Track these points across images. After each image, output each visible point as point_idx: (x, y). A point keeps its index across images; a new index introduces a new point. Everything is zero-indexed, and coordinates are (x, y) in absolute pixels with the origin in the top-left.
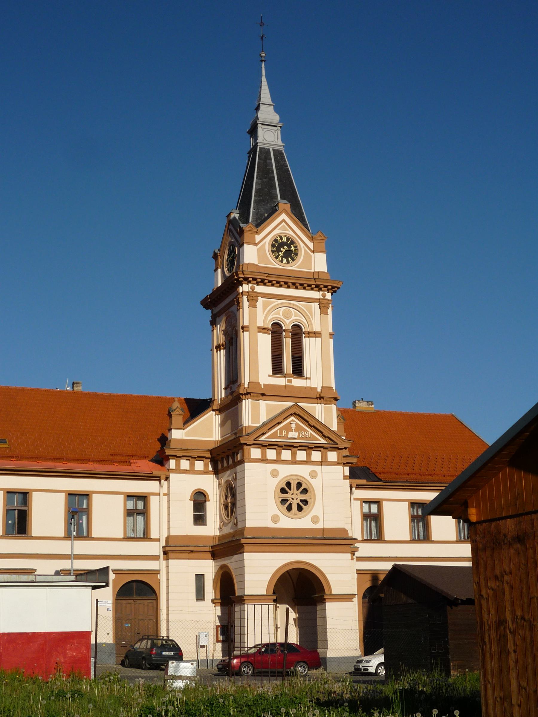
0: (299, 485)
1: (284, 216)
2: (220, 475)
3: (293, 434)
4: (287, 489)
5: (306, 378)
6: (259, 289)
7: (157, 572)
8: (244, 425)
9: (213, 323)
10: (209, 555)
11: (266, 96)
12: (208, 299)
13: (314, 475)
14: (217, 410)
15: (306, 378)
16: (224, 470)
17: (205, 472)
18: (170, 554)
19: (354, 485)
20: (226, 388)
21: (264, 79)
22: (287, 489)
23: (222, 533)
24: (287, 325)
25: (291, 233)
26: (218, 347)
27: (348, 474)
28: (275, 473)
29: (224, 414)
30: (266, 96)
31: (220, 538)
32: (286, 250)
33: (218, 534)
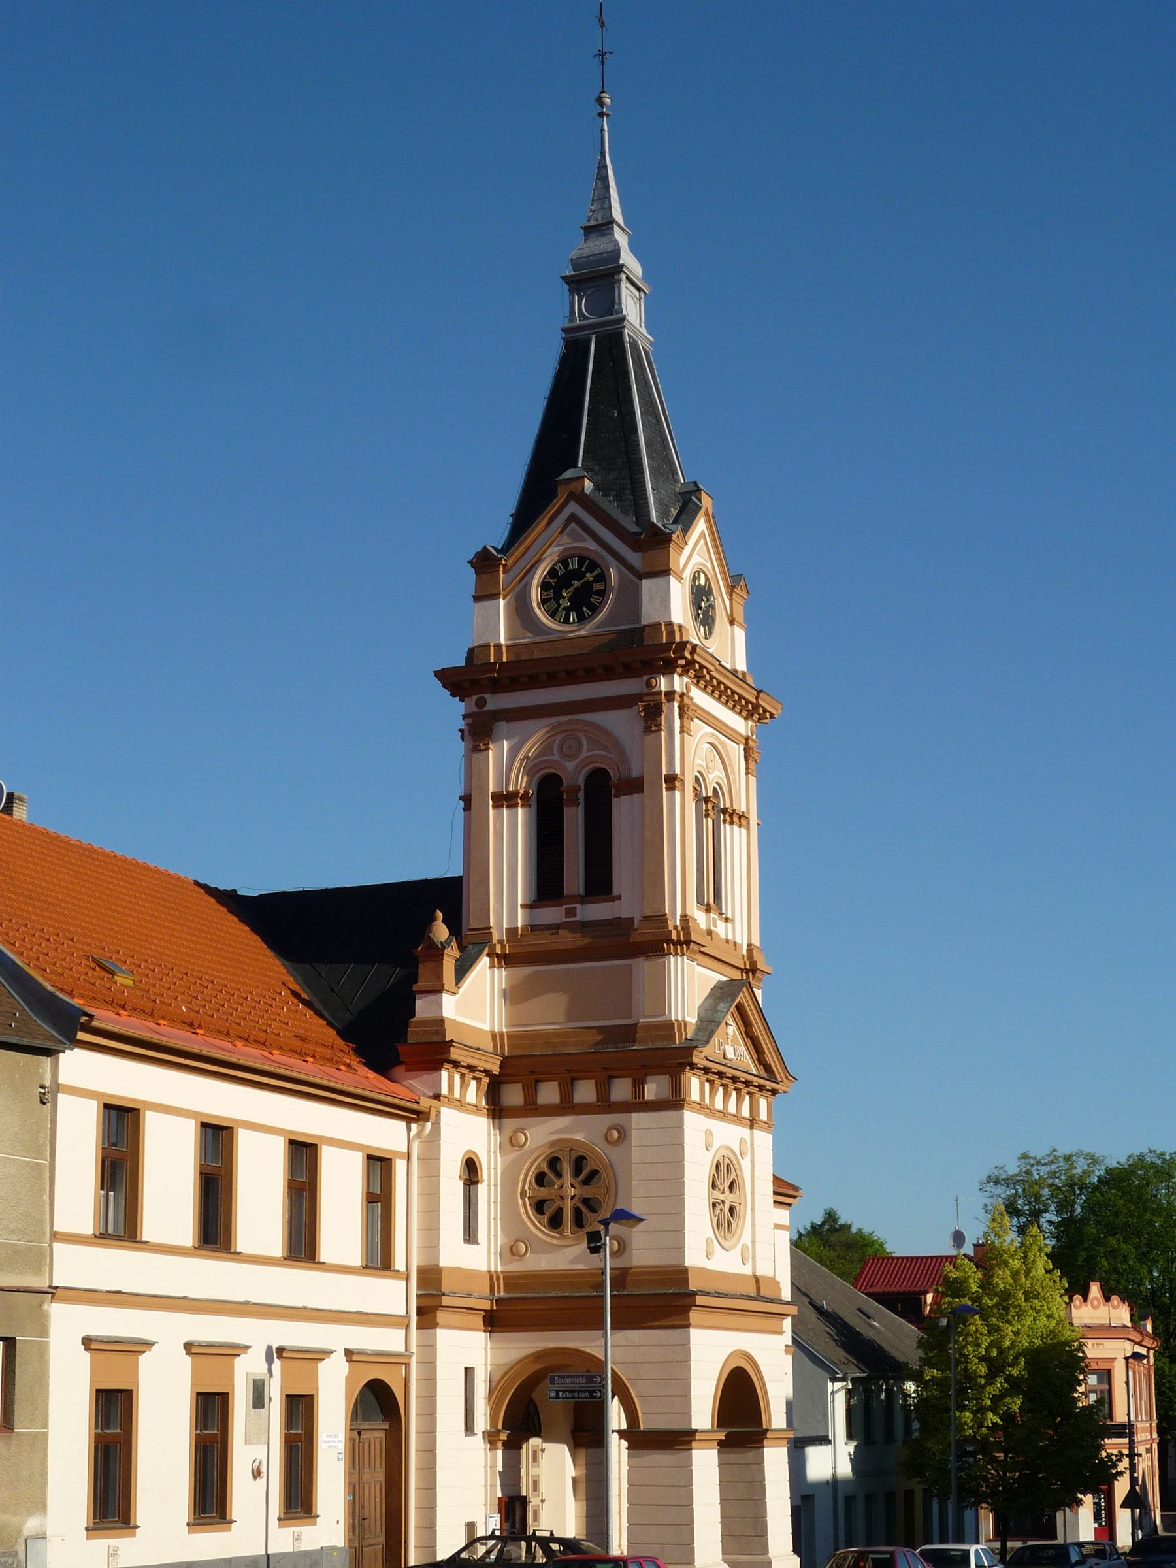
2: (511, 1123)
5: (727, 920)
7: (399, 1360)
8: (673, 1018)
9: (479, 732)
10: (479, 1320)
12: (494, 670)
14: (498, 955)
15: (727, 920)
16: (532, 1109)
17: (474, 1109)
18: (441, 1316)
20: (529, 907)
23: (516, 1267)
26: (505, 799)
29: (523, 971)
31: (511, 1281)
33: (499, 1269)
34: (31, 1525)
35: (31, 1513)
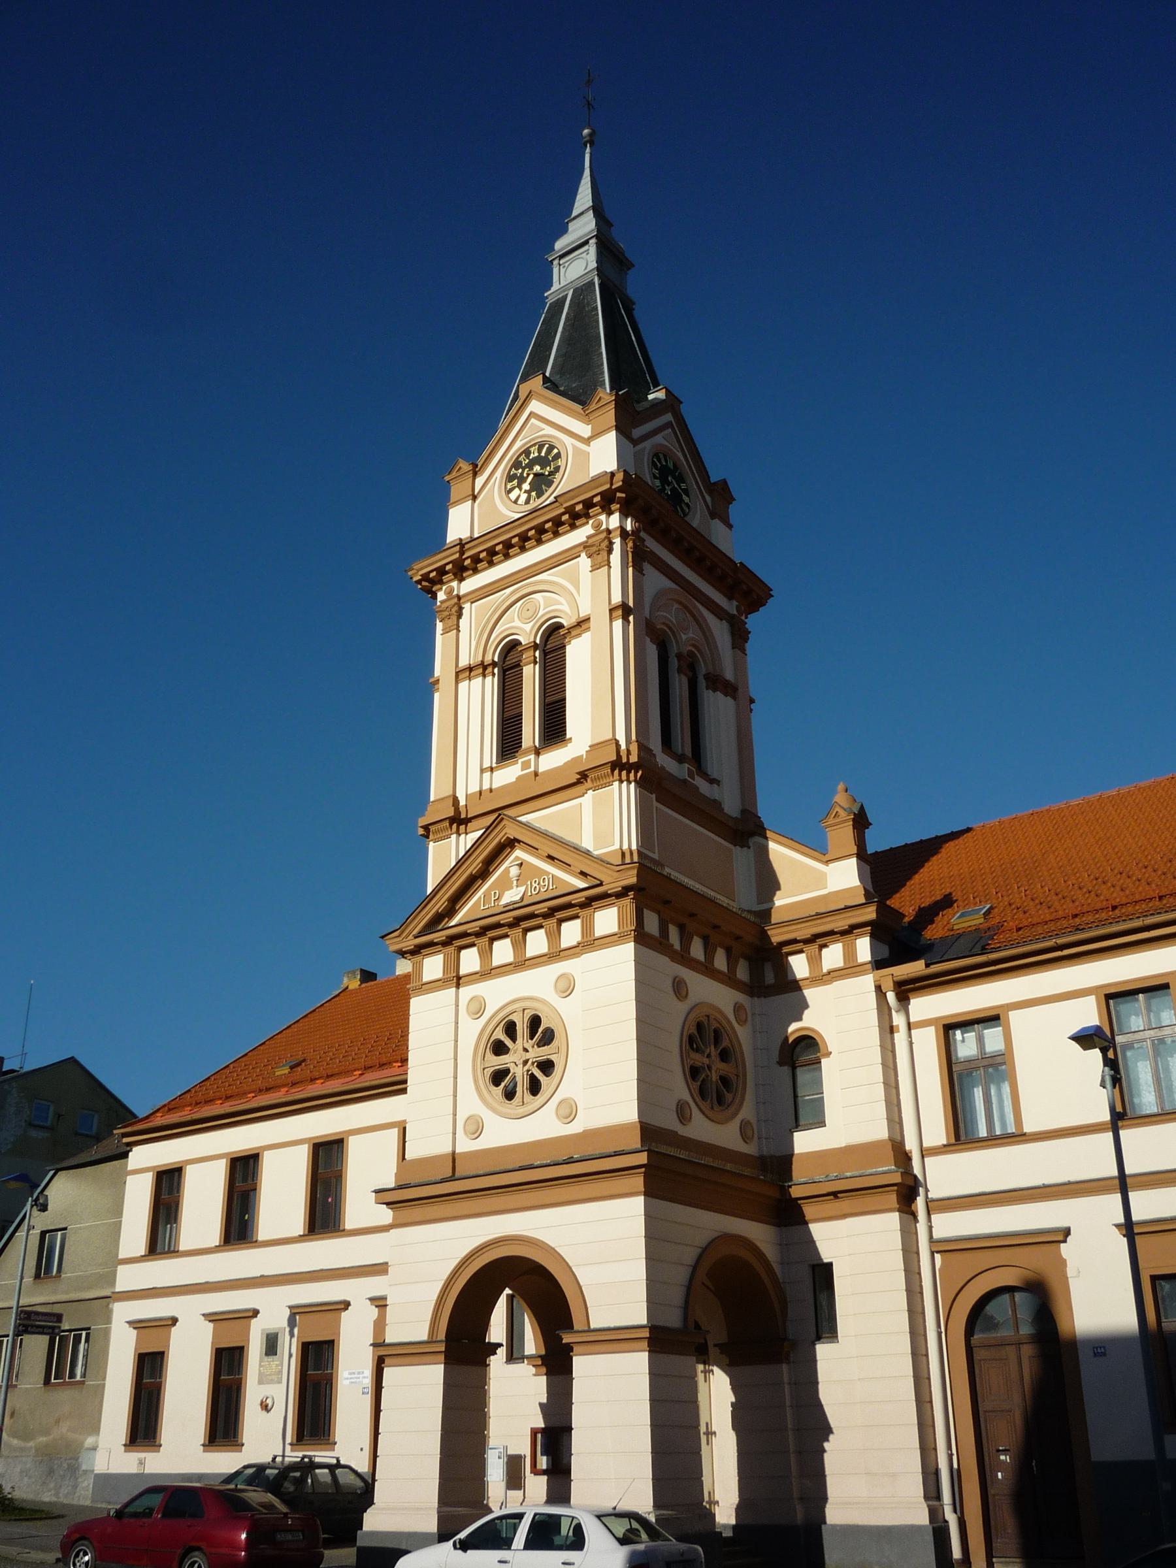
0: (535, 1022)
1: (535, 406)
3: (512, 895)
4: (508, 1042)
6: (472, 583)
11: (584, 197)
13: (567, 987)
19: (888, 985)
21: (587, 172)
22: (508, 1042)
24: (527, 632)
25: (549, 431)
27: (868, 958)
28: (478, 1008)
30: (584, 197)
32: (536, 475)
34: (90, 1441)
35: (90, 1434)
